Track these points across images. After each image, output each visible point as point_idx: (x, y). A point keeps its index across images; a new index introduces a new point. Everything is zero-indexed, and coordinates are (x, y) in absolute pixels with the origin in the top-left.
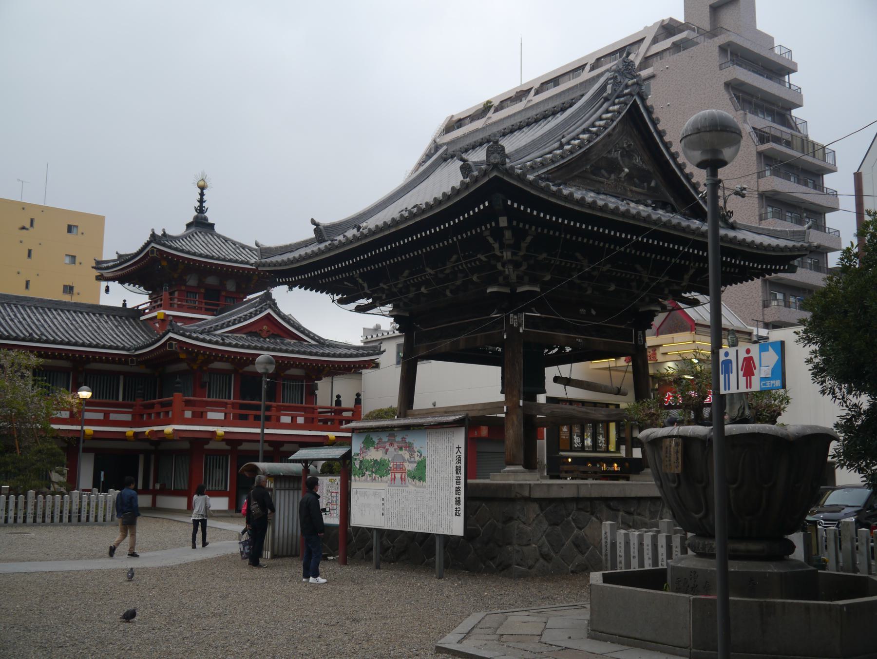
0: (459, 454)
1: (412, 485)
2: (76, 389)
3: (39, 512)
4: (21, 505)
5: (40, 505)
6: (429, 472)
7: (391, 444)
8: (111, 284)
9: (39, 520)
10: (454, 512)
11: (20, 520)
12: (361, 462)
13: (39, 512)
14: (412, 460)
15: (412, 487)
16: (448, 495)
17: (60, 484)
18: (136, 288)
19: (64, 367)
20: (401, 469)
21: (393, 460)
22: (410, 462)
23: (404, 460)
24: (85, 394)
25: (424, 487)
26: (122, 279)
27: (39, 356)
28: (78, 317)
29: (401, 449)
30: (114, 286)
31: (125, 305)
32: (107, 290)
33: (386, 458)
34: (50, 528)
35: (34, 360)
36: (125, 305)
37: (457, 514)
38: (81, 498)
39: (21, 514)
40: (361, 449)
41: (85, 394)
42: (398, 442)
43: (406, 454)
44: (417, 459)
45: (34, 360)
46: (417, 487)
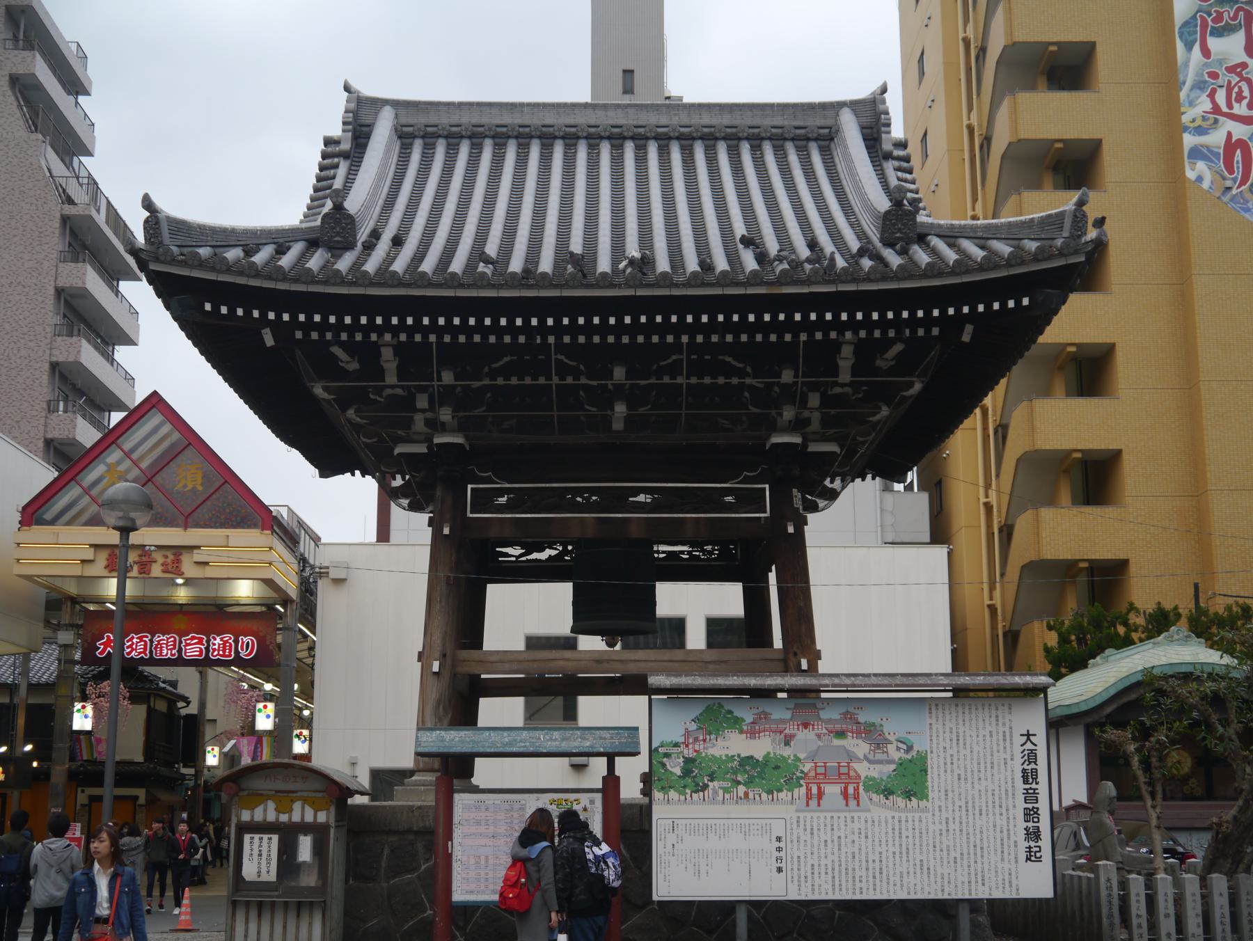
0: (1029, 746)
1: (885, 806)
6: (934, 780)
7: (806, 725)
10: (1023, 856)
12: (688, 761)
14: (879, 756)
15: (879, 814)
16: (1001, 822)
20: (845, 777)
21: (812, 758)
22: (870, 762)
23: (852, 757)
25: (926, 810)
29: (841, 734)
33: (787, 752)
37: (1032, 856)
40: (687, 733)
42: (830, 721)
43: (860, 747)
44: (895, 753)
46: (899, 809)
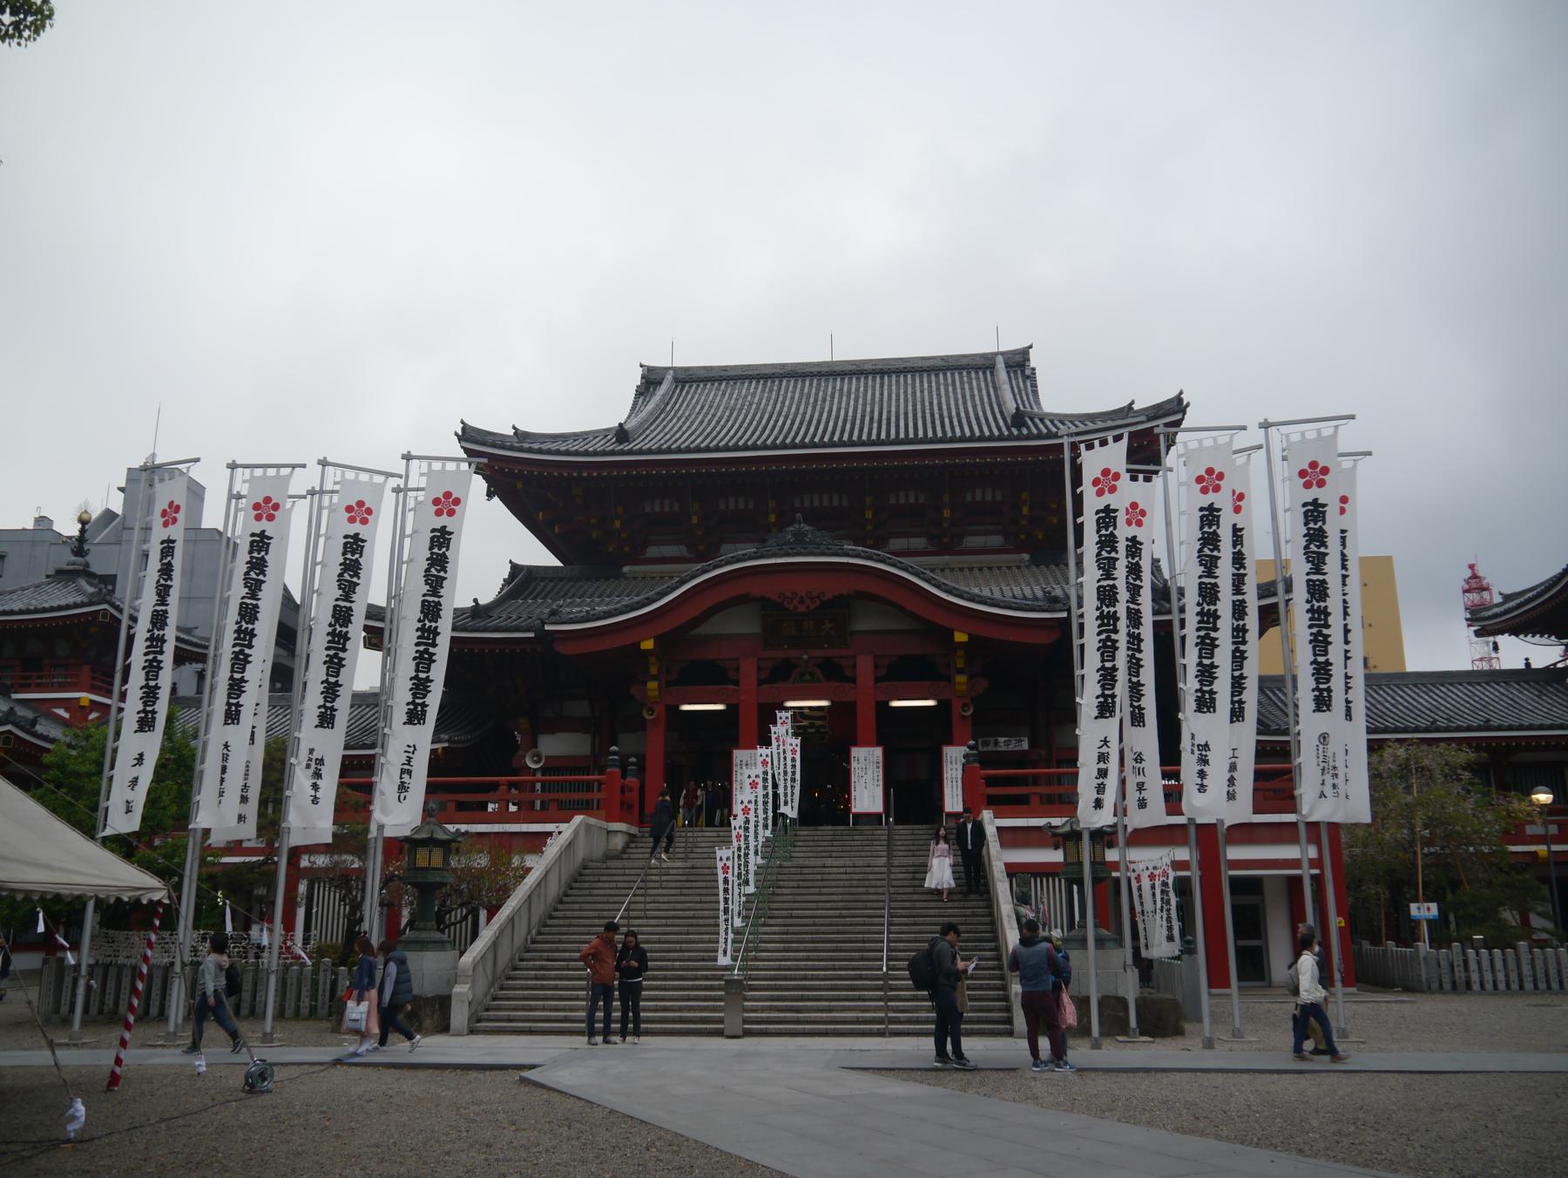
2: (1529, 793)
3: (1540, 974)
4: (1512, 964)
5: (1539, 963)
8: (1500, 639)
9: (1542, 986)
11: (1515, 986)
13: (1540, 974)
17: (1544, 930)
18: (1545, 640)
19: (1503, 764)
24: (1544, 797)
26: (1517, 629)
27: (1478, 749)
28: (1478, 690)
30: (1504, 640)
31: (1528, 665)
32: (1496, 648)
34: (1438, 997)
35: (1468, 755)
36: (1528, 665)
38: (1465, 954)
39: (1514, 977)
41: (1544, 797)
45: (1468, 755)
